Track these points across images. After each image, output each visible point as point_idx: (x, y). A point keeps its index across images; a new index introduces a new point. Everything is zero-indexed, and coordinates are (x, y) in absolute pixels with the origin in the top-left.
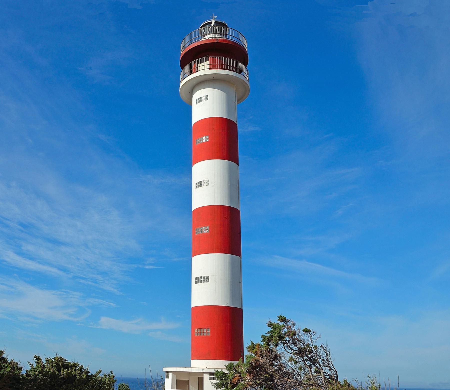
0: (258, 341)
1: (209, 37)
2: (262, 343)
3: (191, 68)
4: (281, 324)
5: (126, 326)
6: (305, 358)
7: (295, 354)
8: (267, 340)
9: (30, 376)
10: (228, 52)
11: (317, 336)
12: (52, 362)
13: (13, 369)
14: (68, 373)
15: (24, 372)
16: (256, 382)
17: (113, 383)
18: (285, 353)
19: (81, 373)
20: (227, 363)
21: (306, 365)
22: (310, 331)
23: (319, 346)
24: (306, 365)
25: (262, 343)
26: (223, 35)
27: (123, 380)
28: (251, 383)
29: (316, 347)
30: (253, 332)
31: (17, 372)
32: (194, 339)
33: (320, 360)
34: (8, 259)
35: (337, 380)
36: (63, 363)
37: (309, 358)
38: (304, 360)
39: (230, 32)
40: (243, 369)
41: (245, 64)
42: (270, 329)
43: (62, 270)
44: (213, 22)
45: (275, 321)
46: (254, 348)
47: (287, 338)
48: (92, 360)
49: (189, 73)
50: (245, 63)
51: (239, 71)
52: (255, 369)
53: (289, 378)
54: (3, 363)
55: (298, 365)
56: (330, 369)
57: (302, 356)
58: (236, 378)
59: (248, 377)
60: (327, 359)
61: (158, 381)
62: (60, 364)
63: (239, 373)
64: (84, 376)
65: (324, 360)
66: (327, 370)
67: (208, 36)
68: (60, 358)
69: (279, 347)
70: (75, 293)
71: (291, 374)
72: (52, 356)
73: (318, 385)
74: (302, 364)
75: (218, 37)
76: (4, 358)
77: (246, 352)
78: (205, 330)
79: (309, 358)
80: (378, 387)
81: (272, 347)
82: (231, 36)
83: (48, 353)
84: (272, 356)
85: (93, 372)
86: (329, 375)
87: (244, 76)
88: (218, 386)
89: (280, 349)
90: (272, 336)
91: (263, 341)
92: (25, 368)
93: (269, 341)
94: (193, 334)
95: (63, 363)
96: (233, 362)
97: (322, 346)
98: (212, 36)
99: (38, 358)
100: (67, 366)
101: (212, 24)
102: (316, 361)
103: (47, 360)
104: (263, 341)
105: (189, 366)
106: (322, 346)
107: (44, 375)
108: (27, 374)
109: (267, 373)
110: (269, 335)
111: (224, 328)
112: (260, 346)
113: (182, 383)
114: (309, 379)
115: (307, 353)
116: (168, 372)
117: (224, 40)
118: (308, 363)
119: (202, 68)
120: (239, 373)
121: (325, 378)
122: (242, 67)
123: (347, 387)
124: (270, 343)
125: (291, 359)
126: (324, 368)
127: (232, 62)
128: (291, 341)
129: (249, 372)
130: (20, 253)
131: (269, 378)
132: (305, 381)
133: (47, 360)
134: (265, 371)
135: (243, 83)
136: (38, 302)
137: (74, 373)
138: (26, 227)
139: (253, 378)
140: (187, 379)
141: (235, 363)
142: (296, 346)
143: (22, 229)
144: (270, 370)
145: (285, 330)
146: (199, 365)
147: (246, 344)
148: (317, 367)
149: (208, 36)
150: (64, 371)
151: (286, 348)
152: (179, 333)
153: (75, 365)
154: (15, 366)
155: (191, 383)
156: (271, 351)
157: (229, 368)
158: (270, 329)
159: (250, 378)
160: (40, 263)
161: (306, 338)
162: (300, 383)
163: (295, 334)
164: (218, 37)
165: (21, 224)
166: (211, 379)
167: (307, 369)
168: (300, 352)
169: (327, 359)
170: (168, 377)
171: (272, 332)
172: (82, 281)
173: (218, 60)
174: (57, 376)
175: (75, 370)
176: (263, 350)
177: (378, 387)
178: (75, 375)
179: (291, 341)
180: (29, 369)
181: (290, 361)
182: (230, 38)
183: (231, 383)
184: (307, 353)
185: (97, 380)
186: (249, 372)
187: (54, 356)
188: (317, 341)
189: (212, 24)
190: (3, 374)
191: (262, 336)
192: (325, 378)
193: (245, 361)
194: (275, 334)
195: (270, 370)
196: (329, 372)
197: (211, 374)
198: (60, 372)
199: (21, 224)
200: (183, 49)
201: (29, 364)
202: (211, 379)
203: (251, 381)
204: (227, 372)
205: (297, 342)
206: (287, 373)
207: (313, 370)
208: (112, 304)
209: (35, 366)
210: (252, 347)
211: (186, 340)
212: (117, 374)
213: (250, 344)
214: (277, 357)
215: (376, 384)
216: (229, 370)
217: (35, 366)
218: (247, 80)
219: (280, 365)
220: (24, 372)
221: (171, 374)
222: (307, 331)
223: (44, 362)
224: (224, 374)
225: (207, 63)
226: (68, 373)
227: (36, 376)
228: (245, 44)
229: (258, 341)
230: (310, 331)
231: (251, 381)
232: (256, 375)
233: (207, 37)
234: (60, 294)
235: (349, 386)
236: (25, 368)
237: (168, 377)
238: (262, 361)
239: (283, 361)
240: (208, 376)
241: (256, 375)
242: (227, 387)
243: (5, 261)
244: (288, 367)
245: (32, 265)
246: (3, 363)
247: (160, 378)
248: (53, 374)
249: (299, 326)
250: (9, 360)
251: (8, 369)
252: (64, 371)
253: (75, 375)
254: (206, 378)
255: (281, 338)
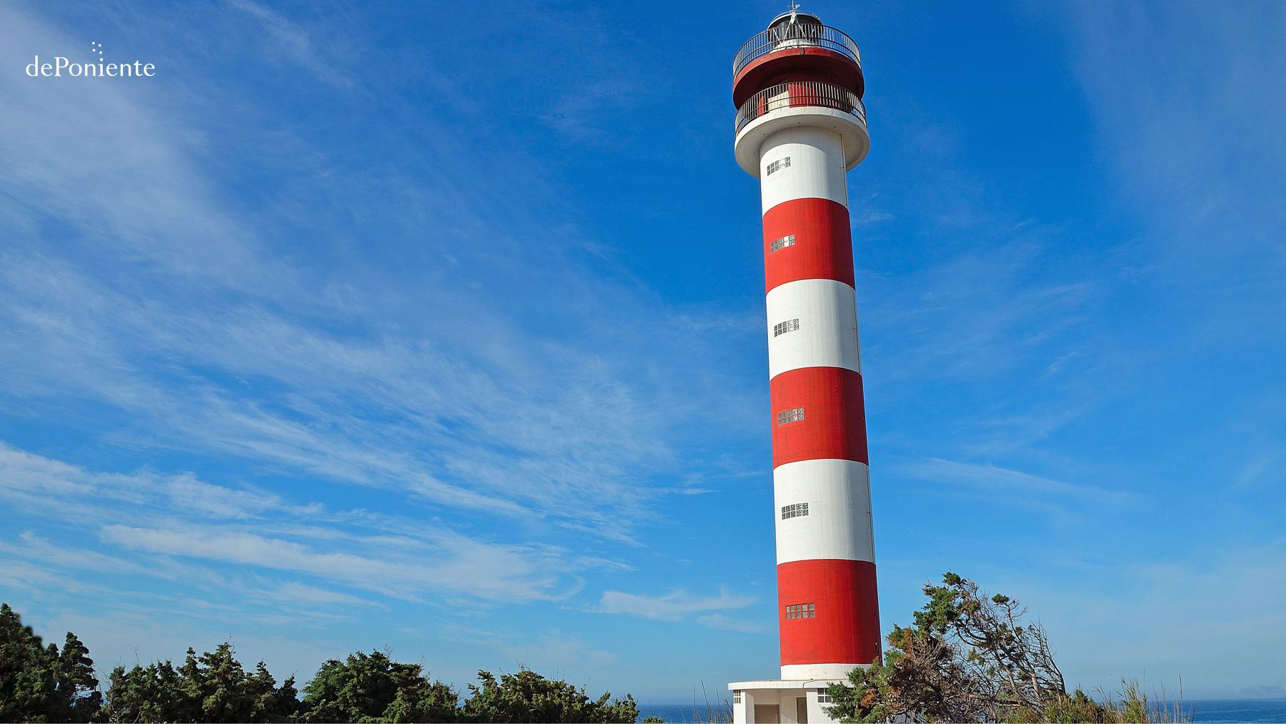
0: (909, 623)
1: (787, 45)
2: (916, 628)
3: (754, 106)
4: (951, 588)
5: (653, 607)
6: (1001, 652)
7: (981, 645)
8: (926, 621)
9: (473, 711)
10: (824, 73)
11: (1021, 608)
12: (515, 683)
13: (440, 699)
14: (545, 703)
15: (461, 704)
16: (907, 703)
17: (634, 716)
18: (960, 644)
19: (572, 700)
20: (851, 667)
21: (1001, 665)
22: (1007, 599)
23: (1025, 628)
24: (1001, 665)
25: (916, 628)
26: (814, 39)
27: (652, 710)
28: (897, 705)
29: (1019, 630)
30: (899, 607)
31: (448, 704)
32: (785, 625)
33: (1028, 655)
34: (420, 490)
35: (1062, 692)
36: (535, 684)
37: (1008, 652)
38: (997, 657)
39: (827, 34)
40: (882, 679)
41: (859, 94)
42: (929, 599)
43: (525, 505)
44: (794, 15)
45: (939, 583)
46: (901, 637)
47: (963, 616)
48: (588, 674)
49: (752, 116)
50: (859, 93)
51: (847, 108)
52: (905, 678)
53: (970, 692)
54: (420, 688)
55: (988, 666)
56: (1049, 671)
57: (994, 649)
58: (869, 697)
59: (892, 694)
60: (1042, 652)
61: (719, 709)
62: (530, 685)
63: (874, 686)
64: (578, 706)
65: (1035, 654)
66: (1043, 674)
67: (785, 44)
68: (530, 673)
69: (949, 633)
70: (553, 548)
71: (974, 683)
72: (514, 672)
73: (1026, 703)
74: (995, 663)
75: (805, 44)
76: (422, 680)
77: (886, 646)
78: (805, 608)
79: (1008, 652)
80: (1142, 700)
81: (935, 633)
82: (828, 41)
83: (506, 667)
84: (937, 652)
85: (593, 698)
86: (1047, 683)
87: (858, 117)
88: (835, 713)
89: (950, 638)
90: (934, 613)
91: (917, 623)
92: (464, 696)
93: (930, 622)
94: (783, 614)
95: (535, 684)
96: (861, 666)
97: (1031, 628)
98: (793, 43)
99: (487, 676)
100: (543, 688)
101: (792, 21)
102: (1021, 656)
103: (505, 679)
104: (917, 623)
105: (777, 677)
106: (1031, 628)
107: (500, 708)
108: (467, 707)
109: (929, 684)
110: (928, 611)
111: (843, 601)
112: (912, 634)
113: (765, 712)
114: (1010, 692)
115: (1003, 643)
116: (738, 691)
117: (816, 50)
118: (1006, 661)
119: (776, 105)
120: (874, 686)
121: (1040, 688)
122: (853, 99)
123: (1082, 704)
124: (932, 627)
125: (973, 656)
126: (1036, 670)
127: (833, 91)
128: (971, 621)
129: (894, 684)
130: (444, 477)
131: (932, 694)
132: (1002, 696)
133: (505, 679)
134: (924, 681)
135: (856, 130)
136: (482, 569)
137: (557, 701)
138: (450, 424)
139: (902, 694)
140: (775, 703)
141: (866, 667)
142: (982, 630)
143: (445, 429)
144: (933, 677)
145: (959, 600)
146: (796, 675)
147: (886, 629)
148: (1023, 668)
149: (785, 44)
150: (538, 699)
151: (963, 635)
152: (758, 615)
153: (558, 686)
154: (443, 694)
155: (782, 709)
156: (934, 642)
157: (855, 677)
158: (929, 599)
159: (896, 695)
160: (483, 494)
161: (999, 613)
162: (993, 699)
163: (977, 607)
164: (805, 44)
165: (443, 421)
166: (821, 700)
167: (1005, 673)
168: (990, 642)
169: (1042, 652)
170: (739, 701)
171: (934, 604)
172: (564, 525)
173: (806, 87)
174: (525, 709)
175: (560, 696)
176: (919, 639)
177: (1142, 700)
178: (561, 705)
179: (971, 621)
180: (471, 697)
181: (971, 659)
182: (826, 45)
183: (860, 707)
184: (1003, 643)
185: (601, 713)
186: (894, 684)
187: (518, 671)
188: (1019, 620)
189: (792, 21)
190: (421, 710)
191: (916, 614)
192: (1040, 688)
193: (884, 663)
194: (941, 608)
195: (933, 677)
196: (1047, 677)
197: (820, 690)
198: (530, 700)
199: (443, 421)
200: (738, 71)
201: (471, 687)
202: (821, 700)
203: (898, 700)
204: (850, 685)
205: (983, 622)
206: (966, 682)
207: (1015, 674)
208: (624, 566)
209: (481, 691)
210: (898, 635)
211: (771, 628)
212: (641, 700)
213: (893, 630)
214: (945, 653)
215: (1138, 696)
216: (854, 682)
217: (481, 691)
218: (863, 125)
219: (953, 668)
220: (461, 704)
221: (743, 694)
222: (1000, 600)
223: (500, 682)
224: (846, 690)
225: (786, 94)
226: (545, 703)
227: (485, 711)
228: (856, 55)
229: (909, 623)
230: (1007, 599)
231: (898, 700)
232: (908, 689)
233: (782, 45)
234: (524, 552)
235: (1086, 701)
236: (464, 696)
237: (739, 701)
238: (917, 662)
239: (957, 660)
240: (816, 695)
241: (908, 689)
242: (852, 715)
243: (415, 493)
244: (968, 671)
245: (467, 499)
246: (420, 688)
247: (722, 703)
248: (518, 706)
249: (985, 591)
250: (432, 683)
251: (432, 700)
252: (538, 699)
253: (561, 705)
254: (812, 698)
255: (951, 616)
